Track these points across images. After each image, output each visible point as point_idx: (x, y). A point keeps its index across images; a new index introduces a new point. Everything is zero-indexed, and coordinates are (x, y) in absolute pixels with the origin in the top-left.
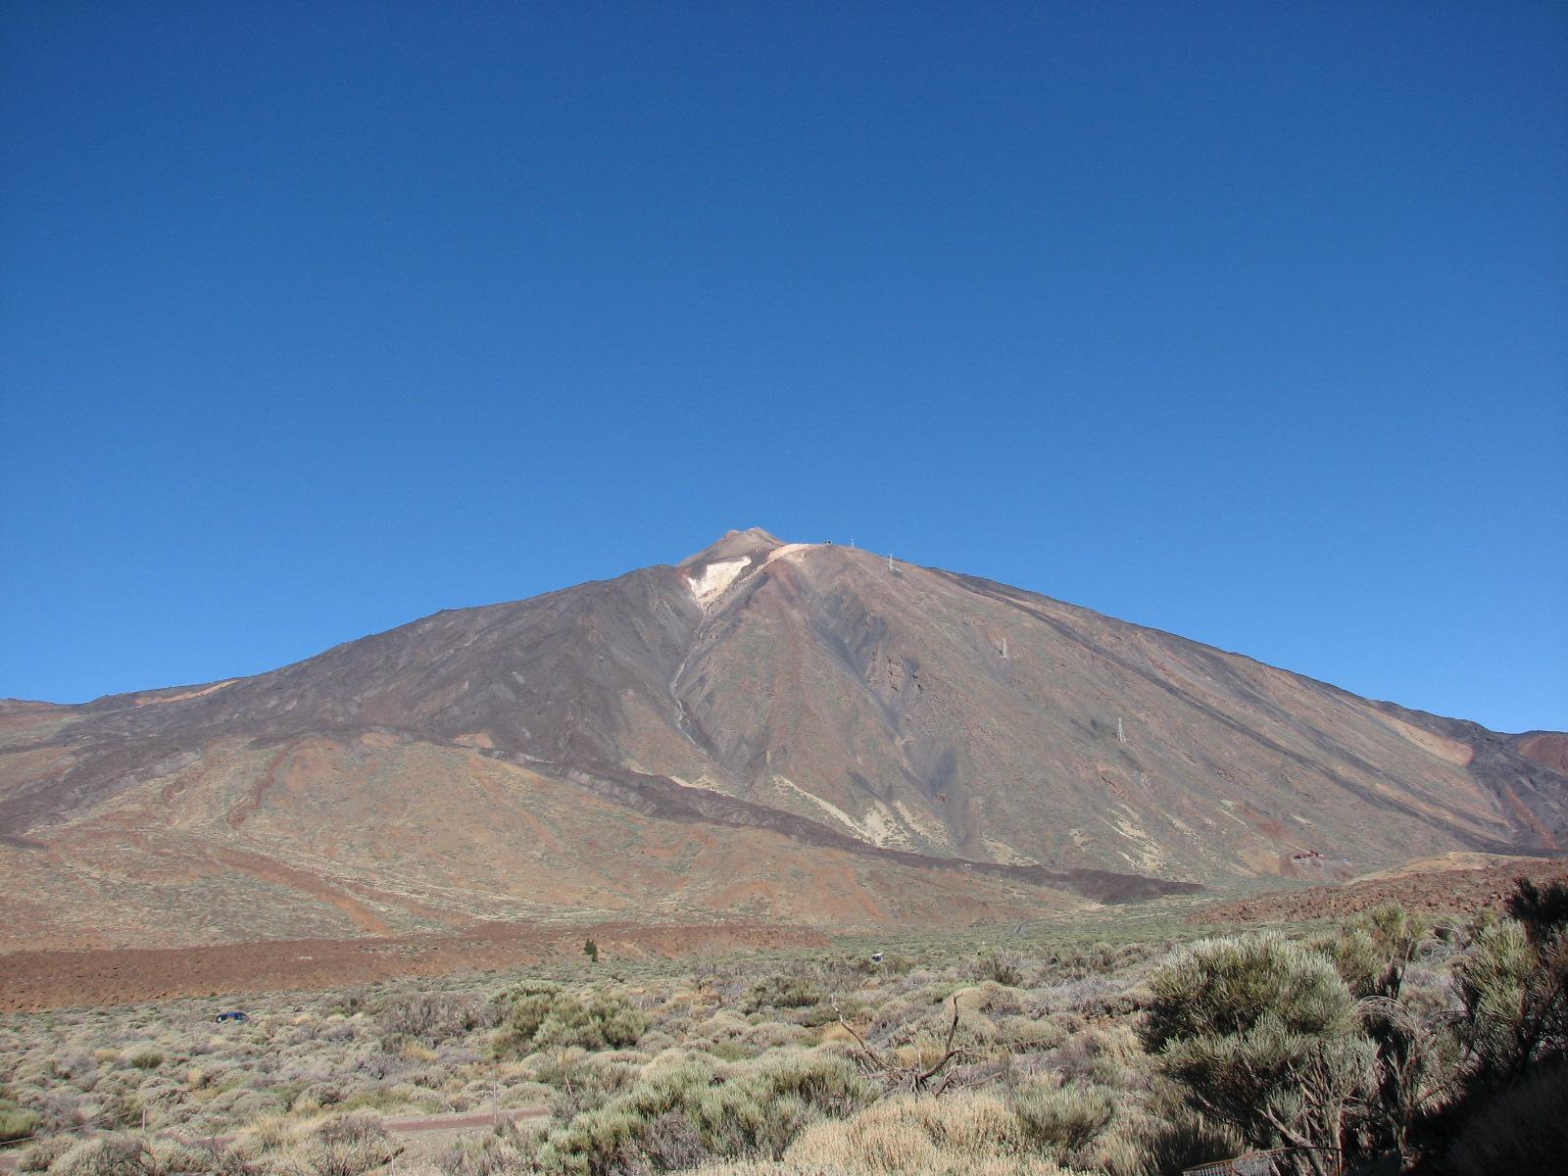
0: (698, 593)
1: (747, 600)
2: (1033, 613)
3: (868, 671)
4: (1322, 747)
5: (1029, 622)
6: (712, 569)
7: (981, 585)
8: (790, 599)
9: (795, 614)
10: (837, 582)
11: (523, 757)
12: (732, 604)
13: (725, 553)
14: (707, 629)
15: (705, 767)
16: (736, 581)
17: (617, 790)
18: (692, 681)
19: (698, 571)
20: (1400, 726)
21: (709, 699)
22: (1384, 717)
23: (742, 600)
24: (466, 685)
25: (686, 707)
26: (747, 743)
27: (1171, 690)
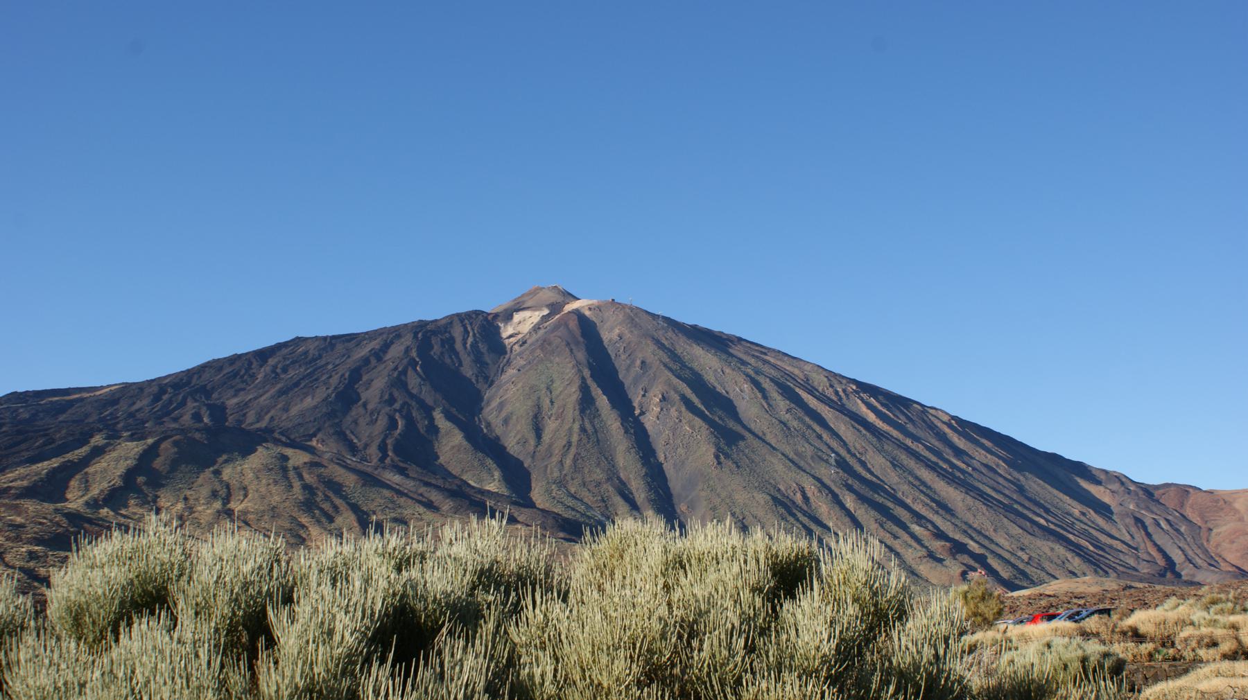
0: (504, 335)
1: (544, 343)
6: (517, 317)
9: (581, 355)
10: (617, 331)
11: (351, 460)
12: (532, 344)
14: (509, 363)
15: (497, 474)
16: (536, 328)
17: (422, 490)
18: (494, 404)
19: (508, 315)
21: (506, 421)
23: (542, 341)
24: (309, 399)
26: (533, 457)
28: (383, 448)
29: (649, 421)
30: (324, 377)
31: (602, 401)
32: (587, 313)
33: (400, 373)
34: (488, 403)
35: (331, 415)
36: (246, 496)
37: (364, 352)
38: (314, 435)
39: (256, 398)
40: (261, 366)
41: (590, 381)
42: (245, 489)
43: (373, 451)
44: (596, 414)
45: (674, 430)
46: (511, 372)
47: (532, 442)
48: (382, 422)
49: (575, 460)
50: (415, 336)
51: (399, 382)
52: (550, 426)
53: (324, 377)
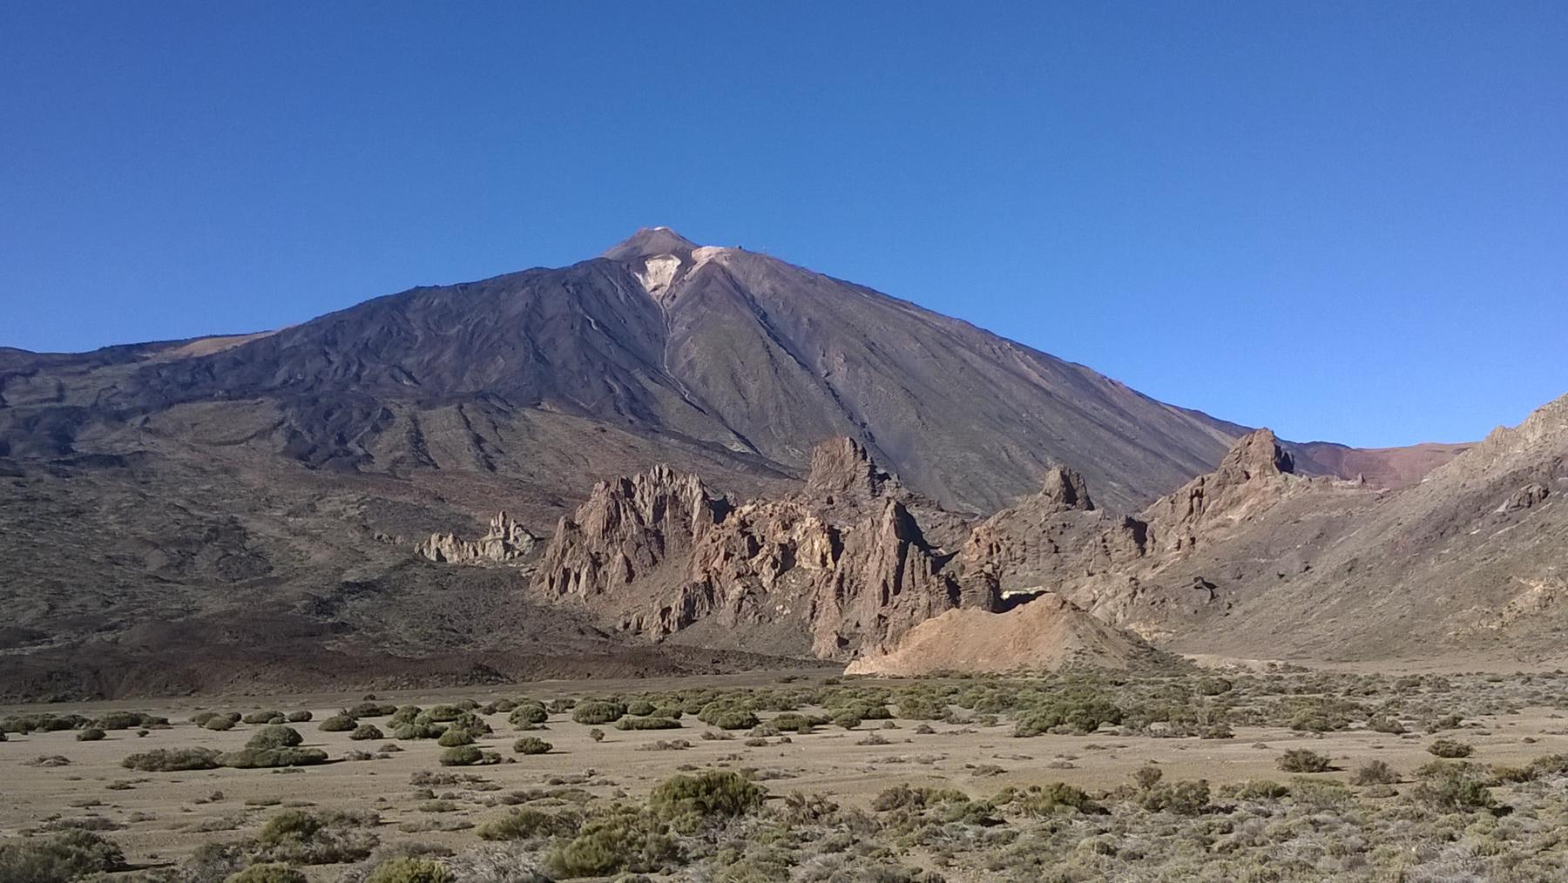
2: (923, 321)
3: (819, 365)
4: (1166, 445)
5: (925, 331)
6: (652, 265)
7: (873, 292)
8: (737, 299)
9: (747, 312)
10: (767, 285)
12: (685, 300)
13: (645, 251)
16: (676, 278)
17: (704, 452)
20: (1214, 433)
21: (704, 380)
22: (1198, 423)
25: (687, 387)
27: (1049, 394)
29: (839, 380)
30: (496, 337)
31: (789, 362)
32: (725, 263)
34: (672, 365)
37: (518, 304)
39: (435, 358)
43: (611, 413)
44: (788, 375)
45: (869, 391)
46: (678, 330)
47: (742, 403)
49: (793, 422)
51: (583, 343)
52: (752, 388)
53: (496, 337)
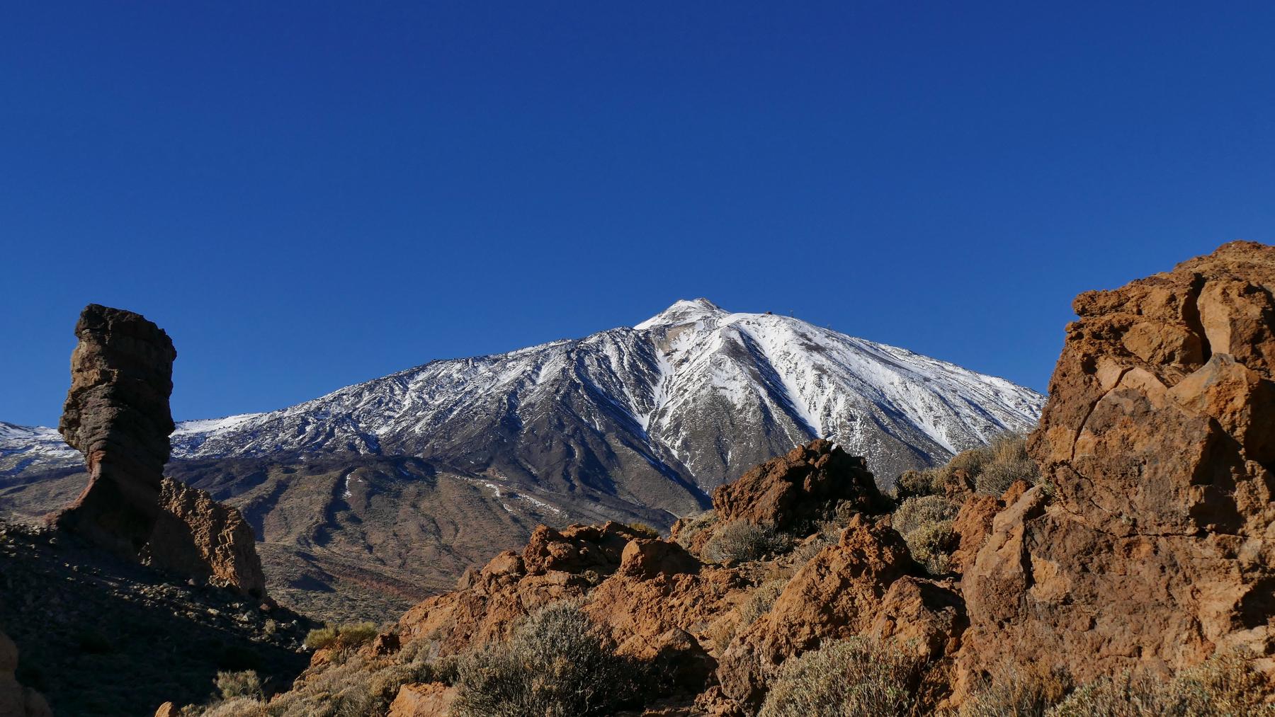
28: (566, 476)
33: (563, 397)
35: (499, 443)
36: (457, 531)
38: (488, 465)
40: (404, 393)
41: (767, 401)
42: (453, 523)
43: (557, 478)
48: (558, 449)
50: (569, 358)
